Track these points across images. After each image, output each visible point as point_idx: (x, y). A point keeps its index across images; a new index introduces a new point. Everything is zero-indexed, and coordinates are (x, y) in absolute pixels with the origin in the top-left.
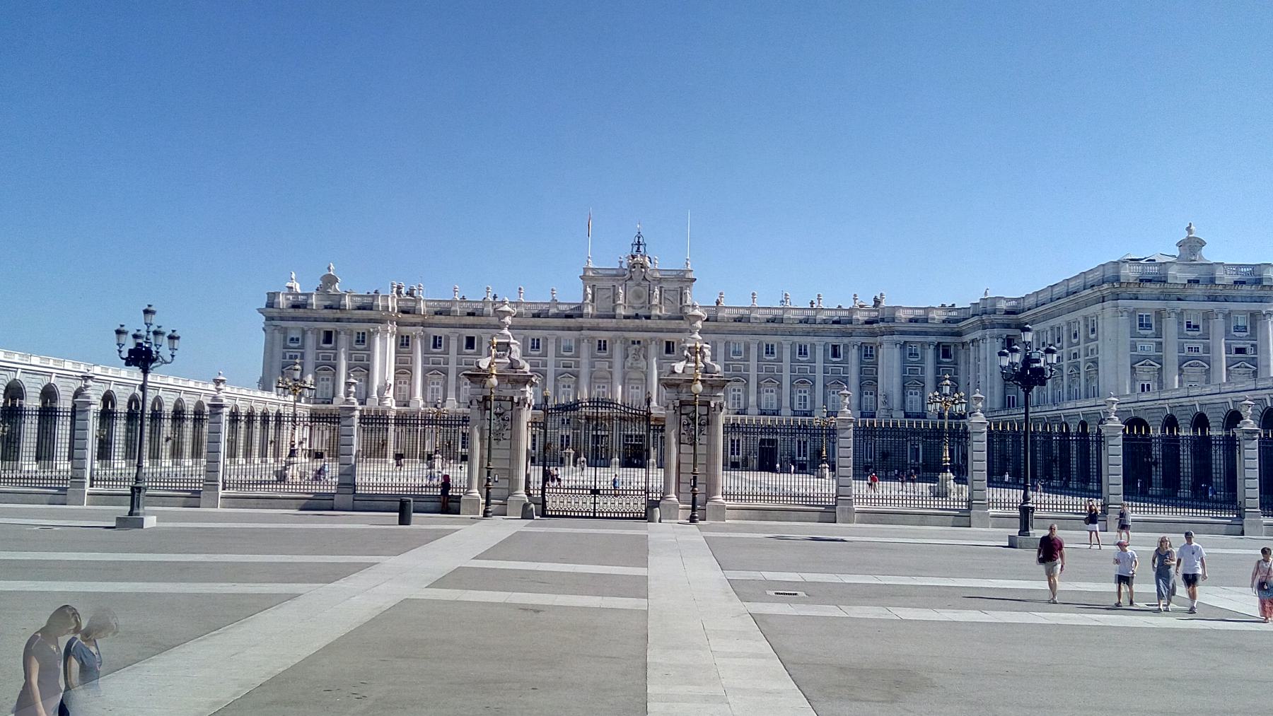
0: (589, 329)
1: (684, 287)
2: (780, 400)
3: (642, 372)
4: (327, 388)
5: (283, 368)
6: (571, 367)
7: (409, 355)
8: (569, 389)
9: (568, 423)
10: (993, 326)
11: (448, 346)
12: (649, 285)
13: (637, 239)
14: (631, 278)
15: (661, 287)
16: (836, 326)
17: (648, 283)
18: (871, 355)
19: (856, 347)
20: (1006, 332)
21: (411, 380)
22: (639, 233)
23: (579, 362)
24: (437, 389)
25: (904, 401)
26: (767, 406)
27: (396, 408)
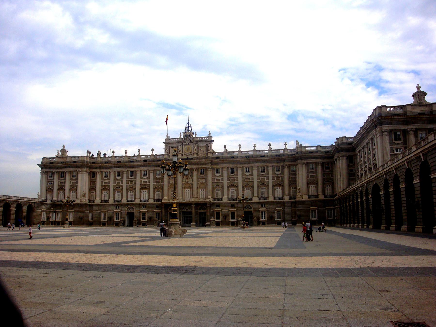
2: (253, 193)
4: (62, 196)
5: (47, 188)
6: (160, 183)
10: (342, 150)
12: (193, 144)
13: (188, 124)
14: (185, 142)
15: (198, 145)
16: (277, 158)
19: (286, 167)
20: (347, 154)
21: (96, 192)
22: (189, 122)
23: (163, 180)
24: (106, 195)
25: (308, 191)
27: (89, 203)
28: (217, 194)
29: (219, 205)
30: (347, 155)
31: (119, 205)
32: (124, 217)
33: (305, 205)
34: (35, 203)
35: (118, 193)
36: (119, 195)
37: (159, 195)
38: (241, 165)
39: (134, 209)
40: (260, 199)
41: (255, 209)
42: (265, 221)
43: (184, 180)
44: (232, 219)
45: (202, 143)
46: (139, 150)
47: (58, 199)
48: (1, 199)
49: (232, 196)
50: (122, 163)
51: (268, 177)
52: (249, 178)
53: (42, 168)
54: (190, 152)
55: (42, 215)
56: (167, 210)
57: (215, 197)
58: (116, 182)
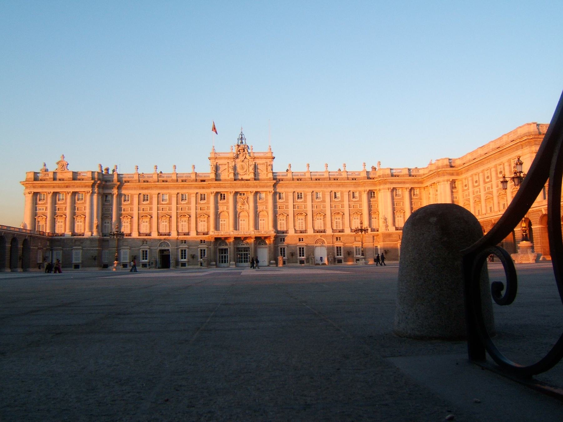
0: (215, 188)
1: (268, 162)
2: (325, 224)
3: (246, 211)
4: (61, 227)
7: (111, 206)
8: (205, 223)
9: (204, 242)
11: (132, 200)
12: (249, 161)
16: (354, 181)
17: (248, 160)
18: (374, 197)
22: (242, 132)
26: (318, 228)
27: (102, 237)
28: (281, 225)
29: (284, 239)
30: (451, 180)
31: (146, 240)
32: (155, 255)
33: (392, 239)
34: (31, 236)
35: (145, 224)
36: (146, 226)
37: (204, 226)
38: (311, 190)
39: (169, 244)
40: (334, 231)
41: (330, 244)
42: (342, 258)
43: (238, 207)
44: (300, 256)
45: (261, 160)
46: (175, 166)
47: (55, 232)
48: (1, 230)
49: (299, 227)
50: (150, 182)
51: (344, 204)
52: (321, 205)
53: (27, 188)
54: (245, 172)
55: (38, 255)
56: (216, 245)
57: (279, 229)
58: (142, 208)
